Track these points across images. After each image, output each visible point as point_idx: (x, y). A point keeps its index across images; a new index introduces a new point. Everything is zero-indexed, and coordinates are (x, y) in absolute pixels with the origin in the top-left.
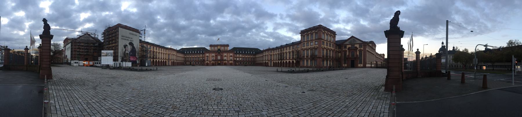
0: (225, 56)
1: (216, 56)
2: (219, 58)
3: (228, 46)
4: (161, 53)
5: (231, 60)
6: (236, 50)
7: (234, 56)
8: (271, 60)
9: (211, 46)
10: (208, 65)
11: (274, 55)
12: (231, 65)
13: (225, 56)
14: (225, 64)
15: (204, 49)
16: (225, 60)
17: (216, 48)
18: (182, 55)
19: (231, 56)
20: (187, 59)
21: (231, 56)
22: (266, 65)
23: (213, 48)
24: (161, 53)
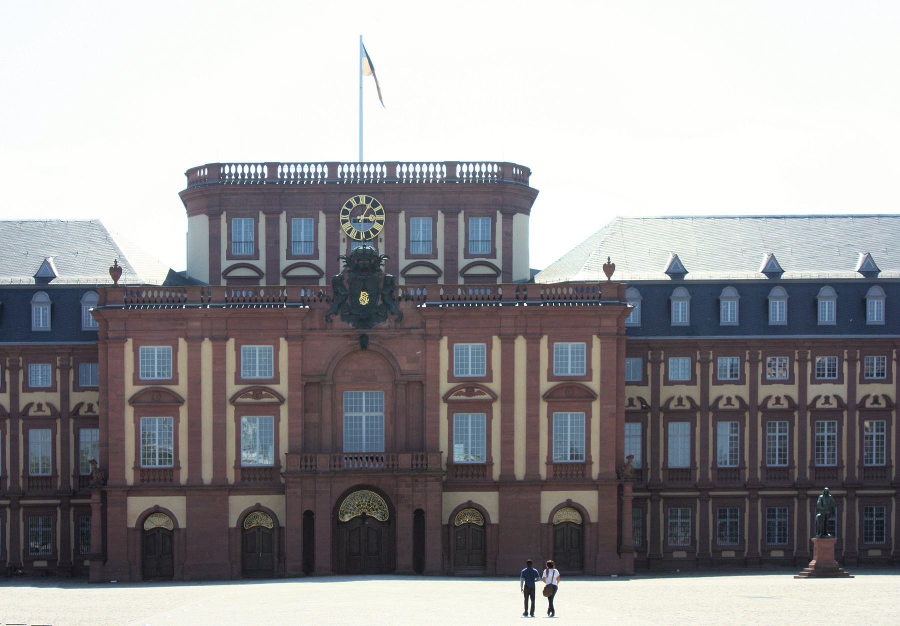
3: (508, 192)
7: (615, 379)
9: (211, 192)
13: (471, 396)
16: (474, 476)
17: (307, 240)
23: (248, 230)
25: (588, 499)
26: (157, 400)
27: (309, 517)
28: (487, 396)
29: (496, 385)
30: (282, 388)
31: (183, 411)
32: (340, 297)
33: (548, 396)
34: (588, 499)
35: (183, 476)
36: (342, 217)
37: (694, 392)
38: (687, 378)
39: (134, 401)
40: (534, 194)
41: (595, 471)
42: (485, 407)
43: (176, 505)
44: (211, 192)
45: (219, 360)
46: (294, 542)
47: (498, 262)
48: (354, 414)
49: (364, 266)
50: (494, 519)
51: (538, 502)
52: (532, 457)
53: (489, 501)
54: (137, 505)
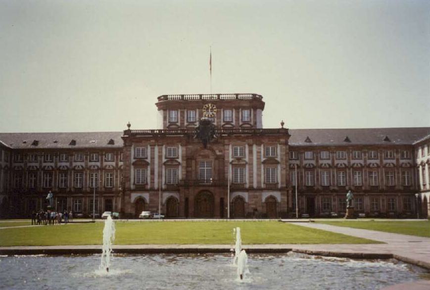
1: (189, 158)
3: (256, 103)
5: (272, 187)
9: (166, 104)
23: (174, 115)
25: (278, 195)
27: (187, 200)
28: (244, 163)
29: (247, 159)
30: (180, 160)
31: (149, 168)
33: (264, 163)
34: (278, 195)
35: (149, 187)
36: (203, 110)
37: (313, 162)
38: (312, 158)
39: (134, 164)
40: (264, 103)
41: (279, 186)
42: (244, 165)
44: (166, 104)
45: (160, 152)
47: (252, 123)
48: (202, 168)
50: (247, 200)
51: (261, 195)
52: (259, 182)
53: (245, 195)
54: (134, 196)
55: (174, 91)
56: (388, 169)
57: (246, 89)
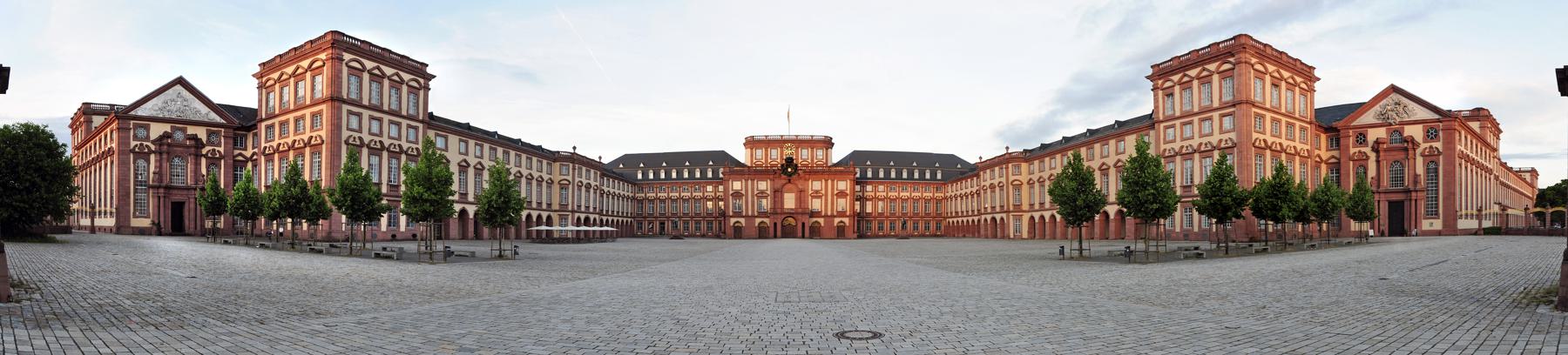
0: (817, 195)
2: (790, 201)
3: (828, 143)
4: (550, 183)
6: (867, 167)
8: (1018, 208)
9: (751, 143)
10: (738, 233)
11: (1030, 183)
12: (841, 233)
13: (817, 195)
14: (815, 233)
15: (721, 158)
16: (818, 214)
17: (776, 157)
18: (625, 190)
19: (842, 194)
20: (648, 208)
21: (842, 194)
22: (996, 230)
23: (760, 153)
24: (540, 182)
25: (846, 220)
26: (737, 195)
32: (784, 169)
34: (846, 220)
43: (742, 220)
46: (772, 230)
49: (790, 161)
53: (821, 221)
54: (733, 220)
55: (760, 132)
56: (927, 201)
57: (819, 132)
